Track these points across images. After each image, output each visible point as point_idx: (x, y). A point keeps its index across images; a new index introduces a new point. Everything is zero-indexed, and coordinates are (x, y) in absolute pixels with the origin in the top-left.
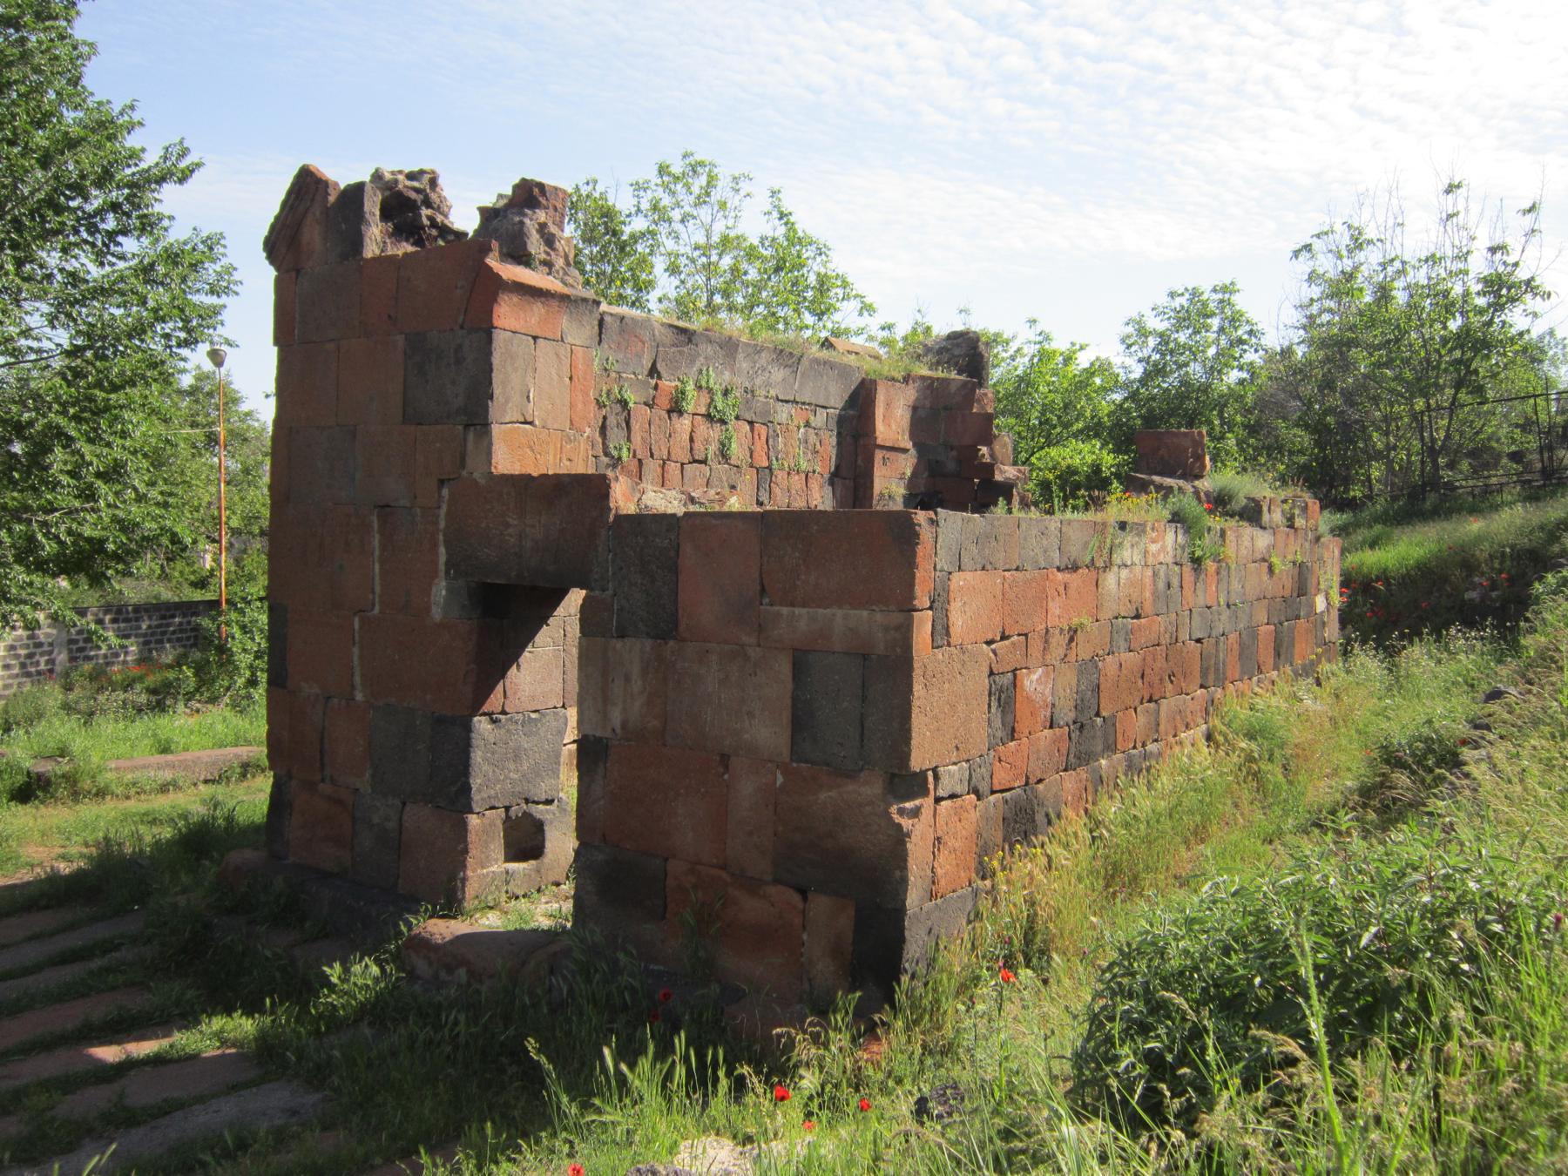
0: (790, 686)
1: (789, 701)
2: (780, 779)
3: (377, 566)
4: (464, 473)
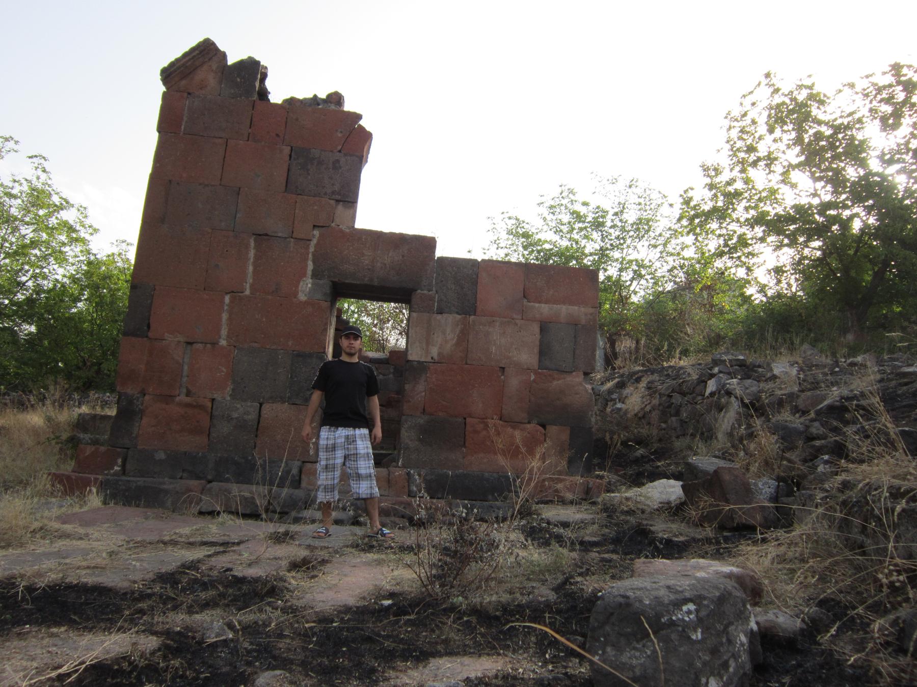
0: (538, 336)
1: (538, 343)
3: (251, 268)
4: (333, 225)
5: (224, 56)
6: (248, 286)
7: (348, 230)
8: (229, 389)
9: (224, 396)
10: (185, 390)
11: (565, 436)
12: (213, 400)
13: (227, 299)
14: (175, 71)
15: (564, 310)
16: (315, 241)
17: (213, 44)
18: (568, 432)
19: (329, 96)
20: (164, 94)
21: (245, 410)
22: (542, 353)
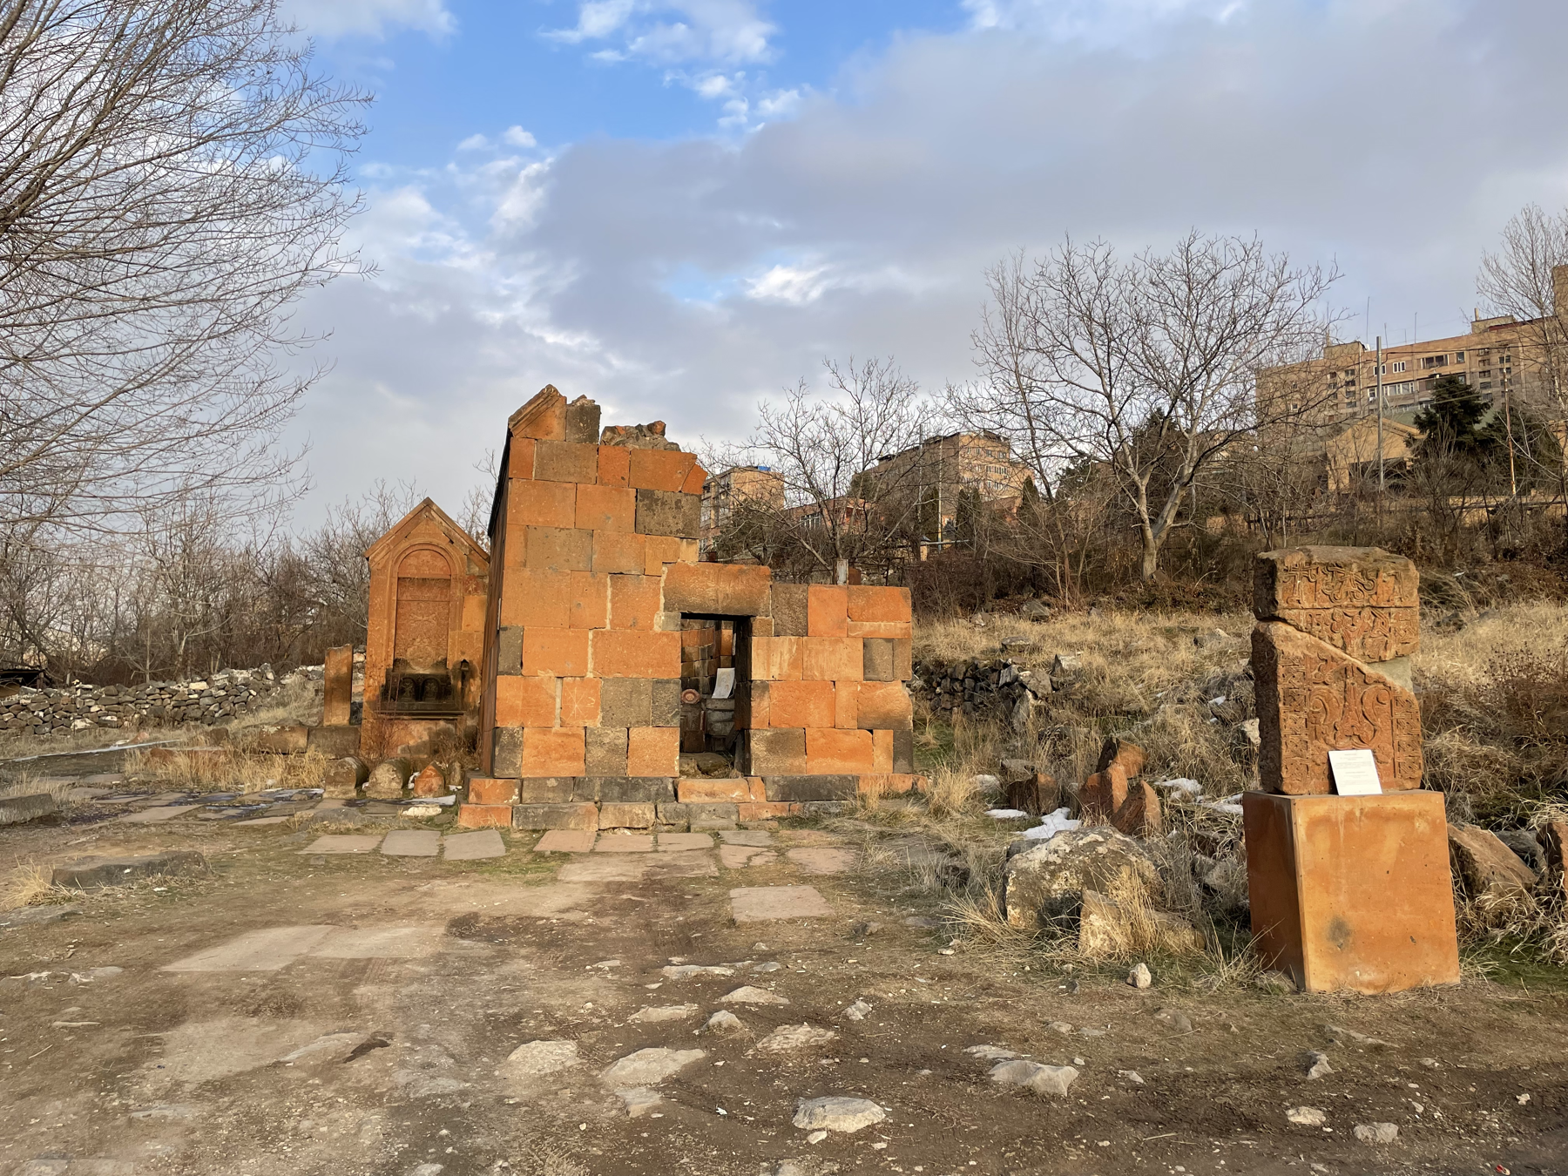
3: (609, 605)
8: (600, 717)
9: (596, 723)
16: (664, 577)
21: (616, 735)
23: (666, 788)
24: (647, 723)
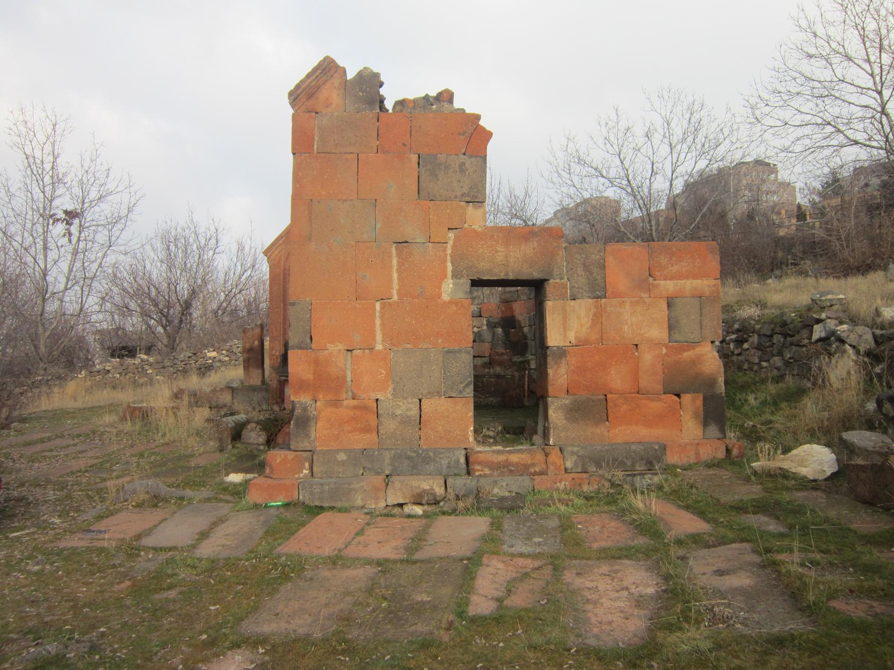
0: (667, 312)
2: (664, 351)
4: (466, 226)
5: (344, 71)
6: (395, 292)
7: (480, 230)
10: (350, 394)
11: (699, 402)
12: (377, 400)
13: (378, 306)
14: (302, 92)
15: (688, 285)
16: (451, 243)
17: (333, 61)
18: (702, 398)
19: (440, 94)
20: (293, 115)
22: (671, 328)
23: (458, 461)
24: (439, 394)
